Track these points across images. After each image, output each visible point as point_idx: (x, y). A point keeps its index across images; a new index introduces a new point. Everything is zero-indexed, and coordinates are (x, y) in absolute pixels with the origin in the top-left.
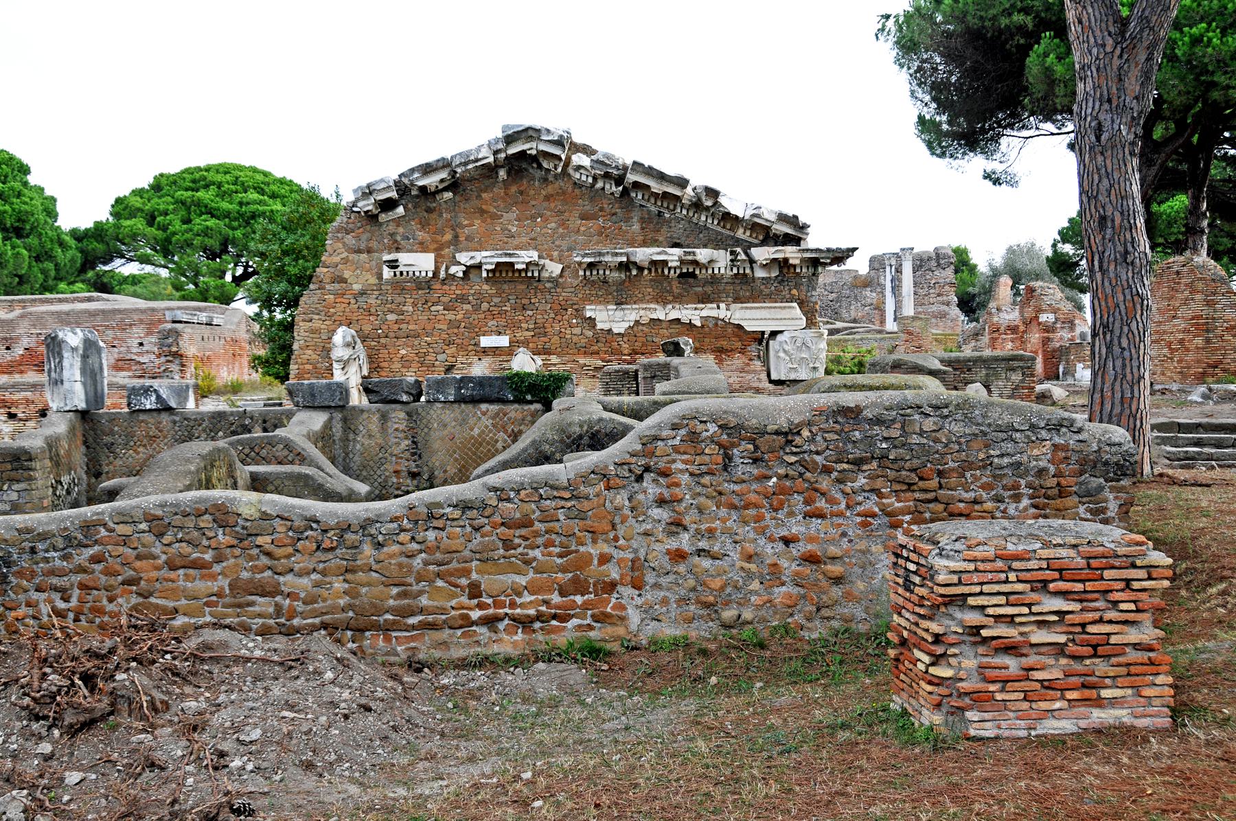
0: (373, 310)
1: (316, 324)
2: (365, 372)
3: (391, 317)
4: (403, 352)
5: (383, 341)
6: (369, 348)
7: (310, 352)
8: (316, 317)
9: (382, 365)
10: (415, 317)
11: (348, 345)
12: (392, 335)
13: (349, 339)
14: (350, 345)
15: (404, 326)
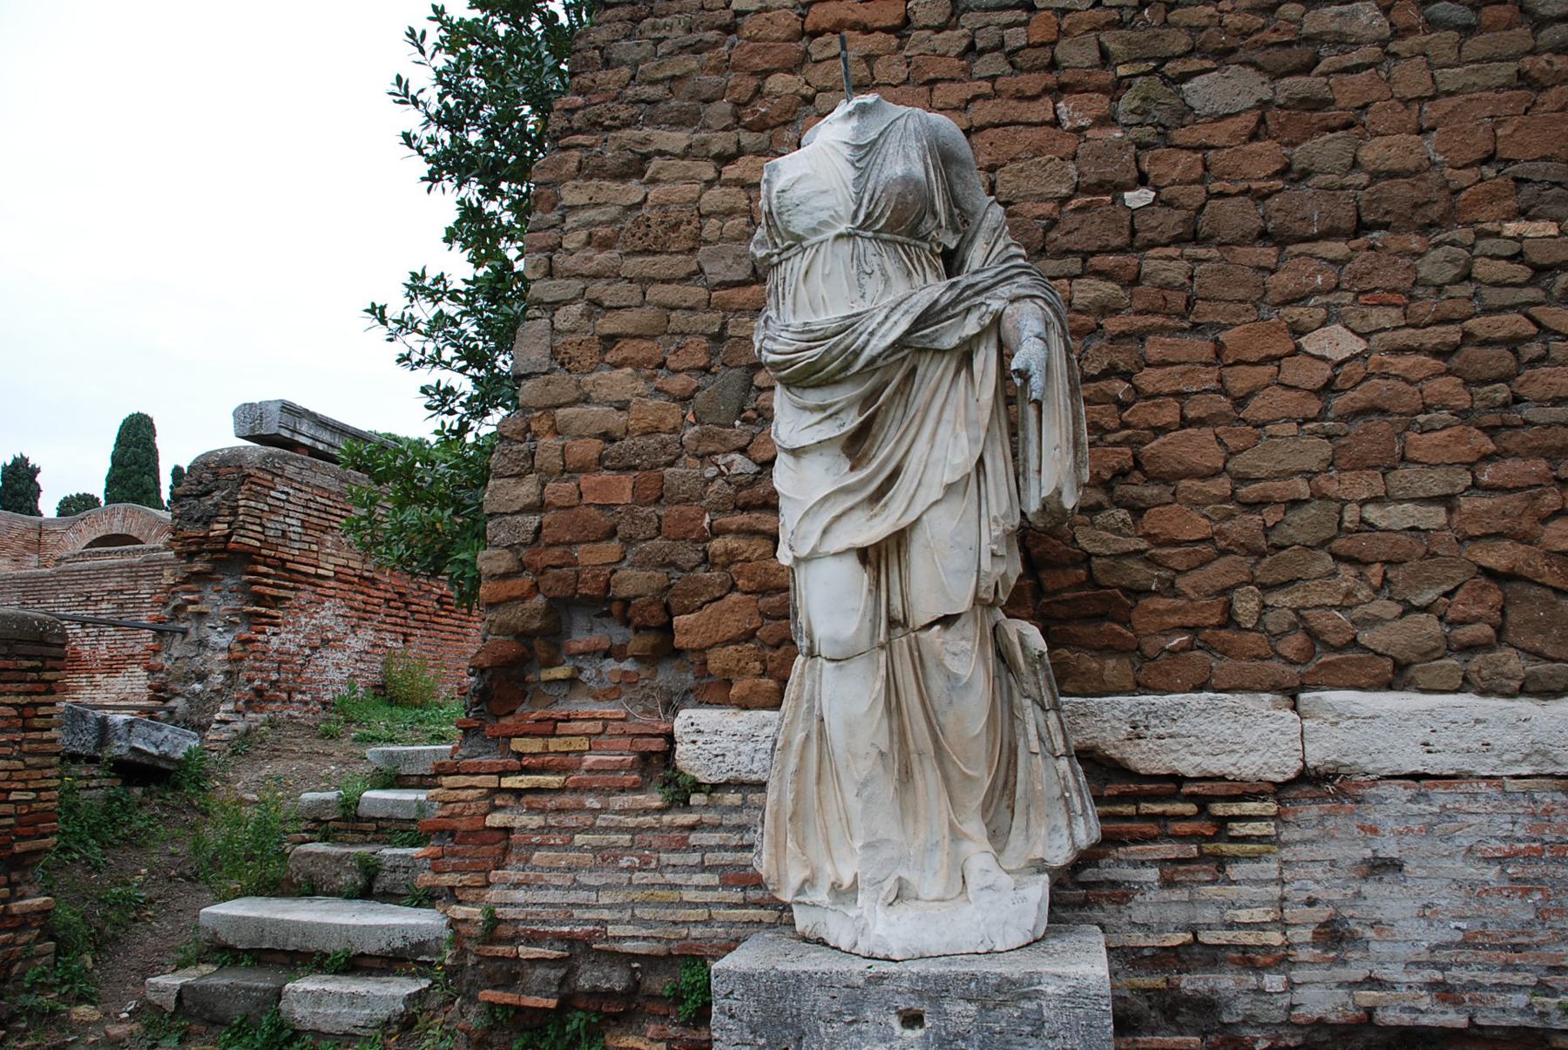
0: (1077, 54)
1: (675, 186)
2: (1056, 471)
3: (1222, 91)
4: (1336, 342)
5: (1165, 266)
6: (1079, 328)
7: (619, 383)
8: (677, 139)
9: (1168, 449)
10: (1411, 77)
11: (904, 224)
12: (1236, 215)
13: (903, 162)
14: (904, 224)
15: (1325, 150)
